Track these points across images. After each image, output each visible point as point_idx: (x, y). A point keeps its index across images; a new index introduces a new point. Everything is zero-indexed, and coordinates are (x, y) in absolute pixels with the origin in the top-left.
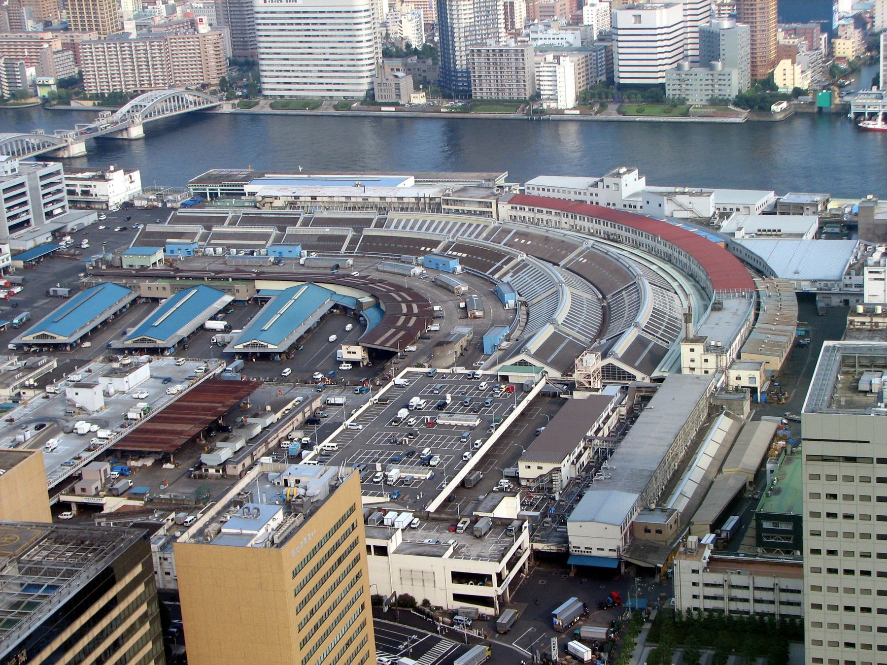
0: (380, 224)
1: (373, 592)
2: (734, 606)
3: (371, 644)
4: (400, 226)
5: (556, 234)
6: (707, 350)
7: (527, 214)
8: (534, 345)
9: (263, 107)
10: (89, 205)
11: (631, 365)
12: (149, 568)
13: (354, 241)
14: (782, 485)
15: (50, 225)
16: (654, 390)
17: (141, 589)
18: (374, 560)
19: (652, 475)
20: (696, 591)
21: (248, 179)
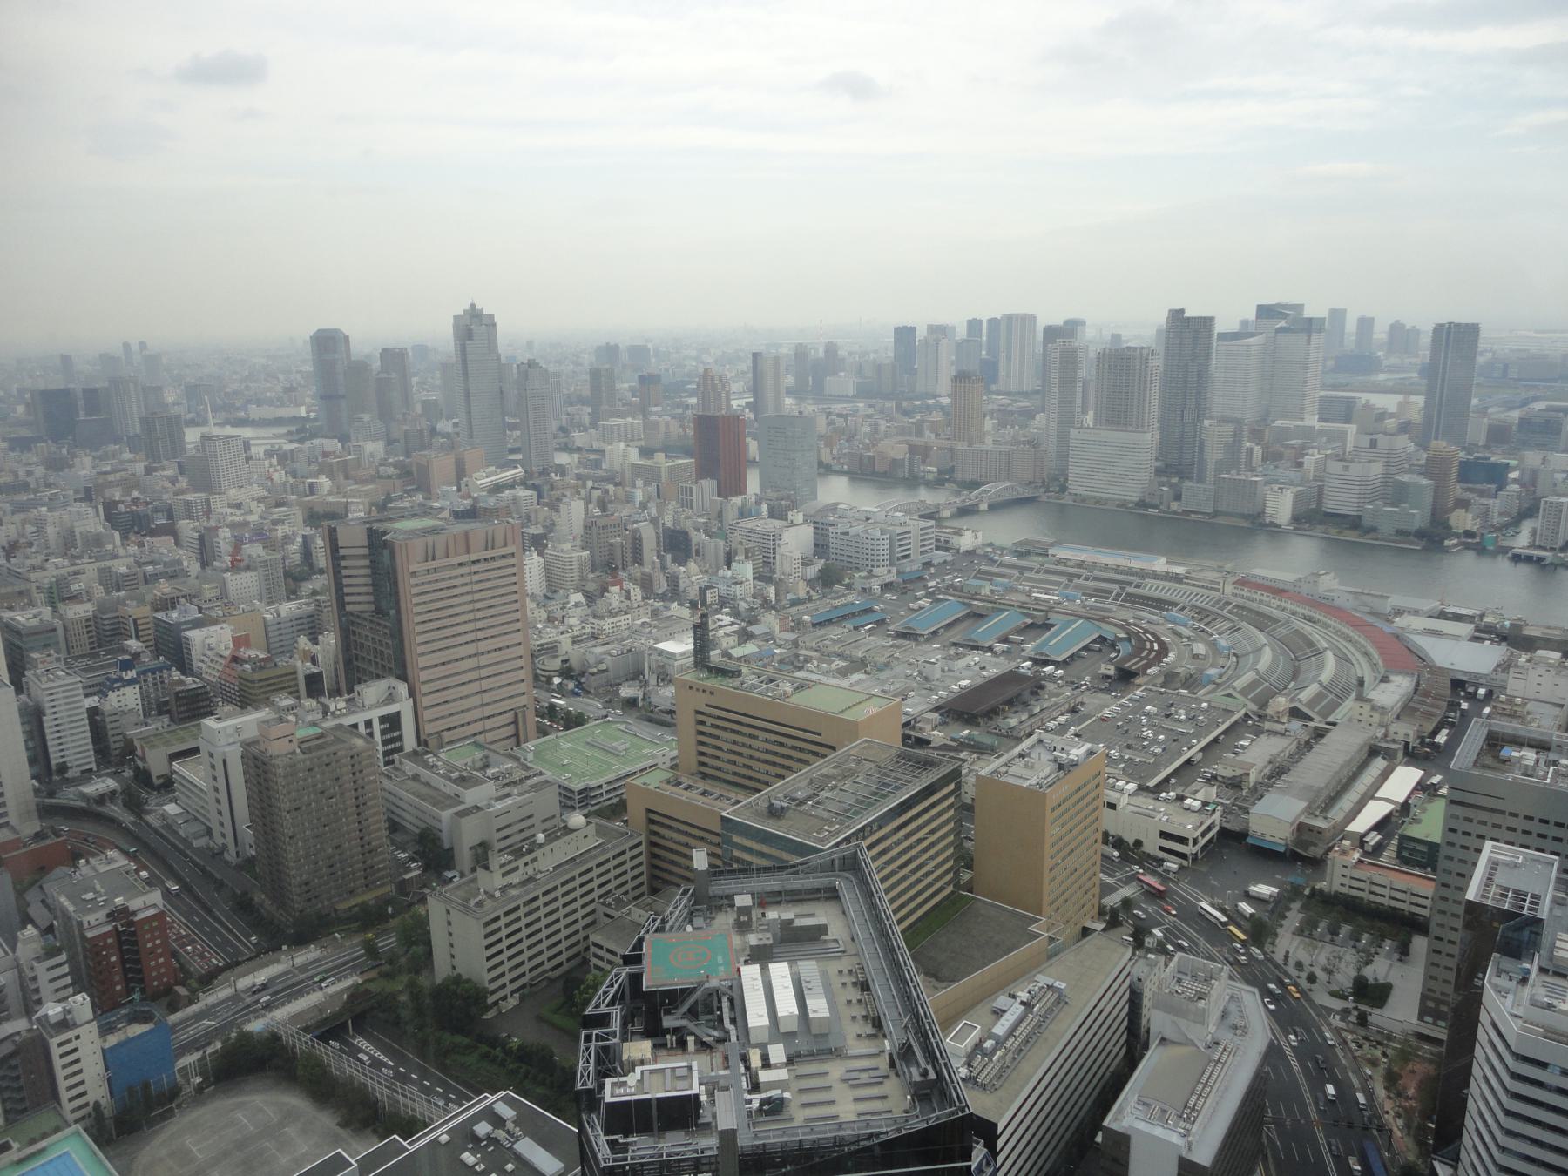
0: (1138, 586)
2: (1372, 898)
3: (1098, 868)
4: (1151, 589)
5: (1264, 609)
6: (1373, 708)
7: (1246, 594)
8: (1240, 683)
9: (1067, 500)
10: (947, 550)
11: (1312, 709)
12: (958, 787)
13: (1119, 595)
14: (1422, 816)
15: (923, 559)
16: (1328, 731)
19: (1319, 791)
20: (1343, 880)
21: (1052, 545)
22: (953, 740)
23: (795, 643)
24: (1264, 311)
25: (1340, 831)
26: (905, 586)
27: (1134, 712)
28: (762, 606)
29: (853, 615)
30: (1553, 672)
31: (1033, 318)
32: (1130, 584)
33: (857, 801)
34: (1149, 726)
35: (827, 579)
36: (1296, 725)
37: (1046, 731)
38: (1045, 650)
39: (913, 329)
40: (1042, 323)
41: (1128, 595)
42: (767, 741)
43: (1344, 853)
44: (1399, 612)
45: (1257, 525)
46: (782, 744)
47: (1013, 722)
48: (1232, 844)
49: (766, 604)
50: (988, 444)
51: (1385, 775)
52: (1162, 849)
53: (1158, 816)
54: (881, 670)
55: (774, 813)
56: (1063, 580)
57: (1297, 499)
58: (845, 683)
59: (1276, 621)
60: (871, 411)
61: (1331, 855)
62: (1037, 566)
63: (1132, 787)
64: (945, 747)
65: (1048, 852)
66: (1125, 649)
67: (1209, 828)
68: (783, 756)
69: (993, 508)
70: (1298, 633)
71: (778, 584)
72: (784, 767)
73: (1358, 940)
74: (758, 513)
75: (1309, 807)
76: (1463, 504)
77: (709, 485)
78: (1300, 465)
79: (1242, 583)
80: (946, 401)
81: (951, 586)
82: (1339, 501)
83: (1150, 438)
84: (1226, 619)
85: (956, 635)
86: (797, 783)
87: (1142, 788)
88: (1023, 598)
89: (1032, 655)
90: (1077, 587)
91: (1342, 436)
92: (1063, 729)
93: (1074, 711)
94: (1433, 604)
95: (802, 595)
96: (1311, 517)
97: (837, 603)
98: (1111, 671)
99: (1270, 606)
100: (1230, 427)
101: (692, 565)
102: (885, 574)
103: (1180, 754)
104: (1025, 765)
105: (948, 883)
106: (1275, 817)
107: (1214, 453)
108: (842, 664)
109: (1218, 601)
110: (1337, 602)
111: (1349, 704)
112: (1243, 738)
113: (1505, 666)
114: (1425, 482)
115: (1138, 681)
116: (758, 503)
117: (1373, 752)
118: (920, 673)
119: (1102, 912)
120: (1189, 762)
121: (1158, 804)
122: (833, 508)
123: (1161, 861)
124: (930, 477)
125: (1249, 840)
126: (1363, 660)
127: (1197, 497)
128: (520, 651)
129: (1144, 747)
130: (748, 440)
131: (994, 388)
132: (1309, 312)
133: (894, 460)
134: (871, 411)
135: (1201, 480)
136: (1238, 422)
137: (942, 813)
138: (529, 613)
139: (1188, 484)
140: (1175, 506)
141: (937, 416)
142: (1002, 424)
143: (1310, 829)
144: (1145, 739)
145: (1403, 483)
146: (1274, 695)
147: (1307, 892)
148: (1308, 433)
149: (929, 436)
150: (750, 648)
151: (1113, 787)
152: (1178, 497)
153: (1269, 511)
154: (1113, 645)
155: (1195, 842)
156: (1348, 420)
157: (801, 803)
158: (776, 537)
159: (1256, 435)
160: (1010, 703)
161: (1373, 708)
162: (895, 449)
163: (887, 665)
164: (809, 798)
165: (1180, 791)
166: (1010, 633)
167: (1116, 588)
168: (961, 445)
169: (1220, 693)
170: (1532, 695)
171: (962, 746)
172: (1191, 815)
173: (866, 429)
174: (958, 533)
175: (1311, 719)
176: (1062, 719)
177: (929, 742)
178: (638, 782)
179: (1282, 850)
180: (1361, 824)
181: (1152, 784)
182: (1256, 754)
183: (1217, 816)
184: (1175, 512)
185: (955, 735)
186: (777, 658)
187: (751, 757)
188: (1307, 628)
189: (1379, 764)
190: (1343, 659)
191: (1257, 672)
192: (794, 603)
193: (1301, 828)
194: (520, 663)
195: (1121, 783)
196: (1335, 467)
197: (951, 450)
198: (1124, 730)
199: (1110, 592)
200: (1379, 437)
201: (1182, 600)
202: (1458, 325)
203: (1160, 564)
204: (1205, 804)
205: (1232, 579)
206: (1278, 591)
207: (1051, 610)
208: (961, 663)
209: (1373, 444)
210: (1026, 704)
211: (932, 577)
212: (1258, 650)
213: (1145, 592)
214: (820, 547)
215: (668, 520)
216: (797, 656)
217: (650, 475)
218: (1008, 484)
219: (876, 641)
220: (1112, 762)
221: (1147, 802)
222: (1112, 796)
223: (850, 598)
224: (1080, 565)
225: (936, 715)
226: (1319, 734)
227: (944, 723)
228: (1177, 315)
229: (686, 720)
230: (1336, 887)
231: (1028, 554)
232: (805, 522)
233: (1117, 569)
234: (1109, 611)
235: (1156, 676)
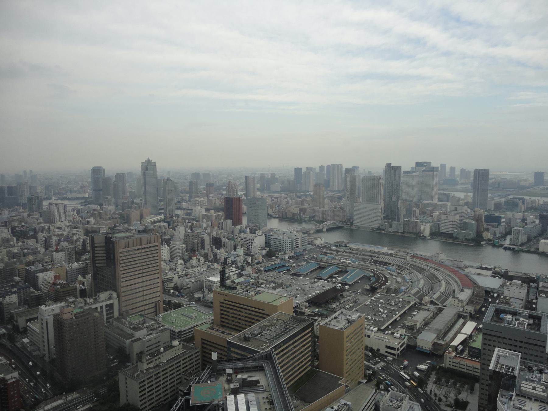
0: (377, 257)
1: (365, 345)
2: (460, 369)
3: (363, 359)
4: (382, 258)
6: (459, 301)
7: (414, 260)
9: (353, 227)
10: (312, 245)
11: (438, 301)
13: (371, 261)
14: (476, 339)
16: (443, 309)
17: (310, 334)
18: (366, 338)
19: (441, 330)
21: (348, 243)
22: (313, 312)
23: (258, 278)
24: (418, 164)
25: (448, 345)
26: (297, 257)
27: (376, 302)
28: (247, 264)
29: (279, 268)
30: (519, 288)
31: (341, 166)
32: (375, 257)
33: (277, 335)
34: (382, 307)
35: (270, 255)
36: (432, 307)
37: (346, 309)
39: (301, 169)
40: (344, 167)
42: (245, 313)
43: (450, 353)
44: (466, 267)
45: (419, 237)
46: (250, 314)
47: (334, 306)
48: (412, 351)
49: (248, 264)
50: (326, 208)
51: (464, 324)
53: (385, 340)
54: (287, 287)
55: (246, 339)
56: (352, 255)
57: (431, 227)
58: (275, 292)
59: (425, 270)
60: (286, 196)
61: (445, 354)
62: (343, 250)
63: (376, 329)
64: (309, 315)
65: (345, 353)
66: (373, 280)
67: (403, 345)
68: (251, 318)
69: (329, 230)
70: (433, 274)
71: (252, 256)
73: (456, 385)
74: (246, 231)
75: (437, 336)
76: (487, 230)
77: (229, 222)
78: (432, 216)
79: (413, 256)
80: (312, 193)
81: (313, 257)
82: (445, 228)
83: (381, 206)
84: (408, 269)
85: (315, 275)
86: (255, 328)
87: (379, 330)
88: (338, 262)
89: (341, 282)
91: (446, 206)
92: (351, 309)
93: (355, 302)
94: (478, 264)
95: (261, 260)
96: (436, 234)
97: (273, 263)
98: (368, 287)
100: (408, 203)
101: (222, 250)
102: (290, 253)
103: (392, 317)
104: (337, 321)
105: (309, 365)
106: (426, 340)
107: (402, 212)
108: (274, 285)
110: (446, 263)
111: (451, 299)
112: (414, 312)
113: (502, 286)
114: (474, 222)
115: (378, 291)
116: (246, 228)
117: (459, 316)
118: (302, 288)
119: (365, 376)
120: (396, 320)
121: (385, 335)
122: (272, 230)
123: (386, 357)
124: (306, 219)
125: (417, 349)
127: (397, 227)
128: (158, 280)
129: (380, 315)
130: (243, 206)
131: (329, 189)
132: (433, 165)
134: (286, 196)
135: (399, 220)
136: (411, 201)
138: (162, 266)
139: (394, 222)
140: (390, 230)
141: (309, 198)
142: (331, 201)
143: (438, 344)
144: (380, 312)
145: (466, 222)
146: (424, 296)
147: (438, 367)
148: (434, 205)
149: (306, 205)
150: (242, 279)
151: (369, 330)
152: (391, 227)
153: (422, 232)
154: (369, 278)
155: (398, 349)
156: (448, 201)
157: (256, 335)
158: (252, 240)
159: (417, 205)
160: (333, 299)
161: (459, 301)
162: (294, 209)
163: (290, 285)
164: (259, 334)
165: (392, 330)
166: (334, 274)
167: (370, 258)
168: (317, 208)
169: (406, 296)
170: (512, 296)
171: (316, 315)
172: (396, 340)
173: (284, 202)
174: (316, 239)
176: (351, 305)
177: (305, 313)
178: (199, 328)
179: (429, 352)
180: (455, 343)
181: (382, 328)
182: (419, 317)
183: (406, 339)
184: (390, 232)
185: (314, 311)
186: (251, 283)
187: (240, 319)
189: (462, 320)
190: (448, 283)
191: (419, 288)
192: (258, 263)
193: (435, 344)
194: (158, 285)
195: (372, 328)
196: (443, 217)
197: (314, 210)
198: (373, 309)
199: (368, 260)
200: (458, 207)
201: (393, 263)
202: (482, 170)
203: (385, 250)
204: (401, 335)
205: (409, 255)
206: (425, 260)
207: (347, 266)
208: (316, 285)
209: (456, 209)
211: (307, 254)
212: (419, 280)
213: (380, 259)
214: (267, 244)
215: (214, 234)
216: (258, 282)
217: (208, 218)
218: (333, 222)
219: (287, 277)
220: (369, 320)
221: (381, 335)
222: (369, 333)
224: (358, 250)
226: (440, 310)
227: (310, 306)
228: (389, 166)
229: (217, 306)
230: (448, 366)
231: (340, 246)
232: (262, 235)
233: (370, 252)
234: (368, 266)
235: (384, 289)
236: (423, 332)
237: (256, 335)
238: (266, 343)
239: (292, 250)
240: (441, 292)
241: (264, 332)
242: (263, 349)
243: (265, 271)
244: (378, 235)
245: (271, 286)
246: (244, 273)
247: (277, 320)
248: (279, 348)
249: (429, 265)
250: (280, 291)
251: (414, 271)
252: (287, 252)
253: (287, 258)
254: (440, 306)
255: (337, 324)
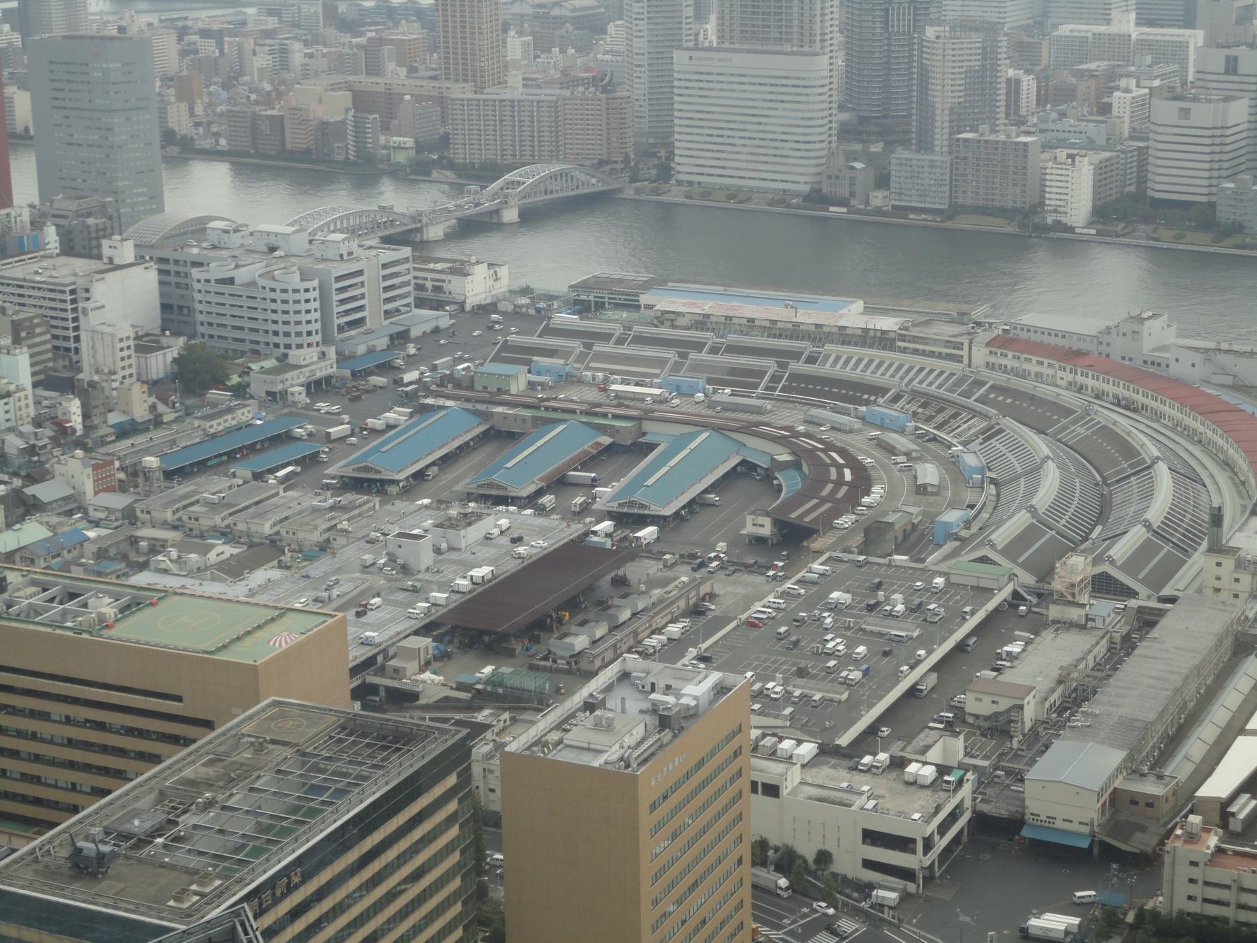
0: (812, 360)
3: (746, 913)
4: (838, 363)
5: (1045, 391)
6: (1240, 565)
7: (1010, 362)
8: (1003, 535)
9: (675, 195)
10: (438, 305)
11: (1134, 575)
13: (776, 379)
16: (1161, 613)
17: (452, 806)
18: (760, 800)
19: (1147, 727)
22: (461, 687)
23: (129, 516)
25: (1186, 799)
26: (350, 385)
27: (810, 604)
28: (55, 441)
29: (252, 448)
32: (796, 355)
33: (262, 829)
34: (837, 630)
35: (194, 378)
36: (1104, 608)
37: (644, 655)
38: (638, 497)
41: (794, 377)
42: (68, 721)
43: (1191, 838)
45: (1030, 231)
46: (101, 726)
47: (580, 641)
48: (998, 840)
49: (63, 435)
50: (515, 89)
52: (868, 864)
53: (859, 802)
54: (310, 558)
55: (86, 868)
56: (670, 354)
57: (1102, 172)
58: (238, 590)
59: (1068, 412)
60: (271, 22)
61: (1169, 845)
62: (618, 330)
63: (808, 749)
64: (445, 704)
65: (648, 891)
66: (789, 483)
67: (953, 816)
68: (105, 749)
69: (532, 217)
70: (1107, 433)
72: (106, 771)
74: (38, 245)
75: (1130, 758)
78: (1105, 109)
79: (1004, 342)
81: (451, 379)
82: (1177, 177)
83: (826, 65)
84: (975, 413)
85: (463, 478)
86: (134, 801)
87: (827, 752)
88: (593, 395)
89: (614, 507)
90: (697, 368)
91: (1182, 47)
92: (674, 649)
93: (696, 612)
95: (140, 412)
96: (1130, 209)
97: (216, 426)
98: (766, 528)
99: (1055, 382)
100: (975, 39)
102: (315, 361)
103: (896, 678)
104: (600, 723)
106: (1071, 782)
107: (946, 95)
108: (229, 550)
109: (959, 383)
110: (1175, 369)
111: (1199, 559)
112: (1012, 640)
115: (817, 545)
116: (37, 223)
118: (392, 559)
120: (913, 692)
121: (858, 777)
122: (197, 228)
123: (866, 889)
124: (401, 158)
125: (1026, 833)
126: (1222, 477)
127: (921, 177)
129: (829, 672)
130: (10, 90)
133: (324, 125)
134: (271, 22)
135: (925, 144)
136: (989, 30)
137: (437, 838)
139: (901, 153)
140: (878, 199)
141: (409, 31)
142: (542, 45)
143: (1134, 799)
144: (832, 654)
146: (1063, 552)
147: (1130, 918)
148: (1117, 46)
149: (395, 74)
150: (32, 531)
151: (773, 754)
152: (882, 182)
153: (1051, 201)
154: (768, 477)
155: (928, 844)
156: (1189, 23)
157: (144, 841)
158: (78, 294)
159: (1025, 54)
160: (573, 604)
161: (1240, 565)
162: (325, 101)
163: (324, 547)
165: (896, 748)
166: (571, 465)
167: (770, 365)
168: (460, 91)
169: (966, 557)
171: (481, 698)
172: (919, 792)
173: (262, 60)
174: (460, 270)
175: (1133, 594)
176: (675, 629)
177: (415, 696)
179: (1085, 844)
180: (1219, 785)
181: (844, 740)
182: (1035, 666)
183: (967, 789)
184: (879, 211)
185: (466, 678)
186: (90, 549)
187: (37, 758)
188: (1122, 423)
190: (1186, 476)
191: (1032, 510)
192: (126, 431)
193: (1117, 800)
195: (787, 744)
196: (1166, 112)
197: (442, 101)
198: (792, 643)
199: (760, 374)
200: (1242, 52)
203: (852, 314)
204: (943, 770)
205: (983, 336)
206: (1071, 356)
207: (647, 415)
208: (472, 534)
209: (1231, 66)
210: (603, 606)
211: (412, 362)
212: (1034, 471)
213: (824, 369)
214: (175, 312)
216: (134, 541)
218: (556, 167)
219: (302, 500)
220: (770, 704)
221: (836, 776)
222: (769, 770)
223: (245, 413)
224: (702, 322)
225: (425, 642)
226: (1147, 621)
227: (443, 656)
230: (1181, 904)
231: (600, 306)
232: (140, 260)
233: (772, 329)
234: (758, 411)
235: (850, 532)
236: (1057, 744)
237: (144, 841)
238: (205, 879)
239: (326, 341)
240: (1147, 525)
241: (187, 820)
242: (187, 915)
243: (169, 475)
244: (812, 232)
245: (212, 557)
246: (43, 491)
247: (259, 747)
248: (277, 901)
249: (1089, 382)
250: (268, 585)
251: (1008, 421)
252: (295, 356)
253: (299, 394)
254: (1145, 599)
255: (597, 739)
